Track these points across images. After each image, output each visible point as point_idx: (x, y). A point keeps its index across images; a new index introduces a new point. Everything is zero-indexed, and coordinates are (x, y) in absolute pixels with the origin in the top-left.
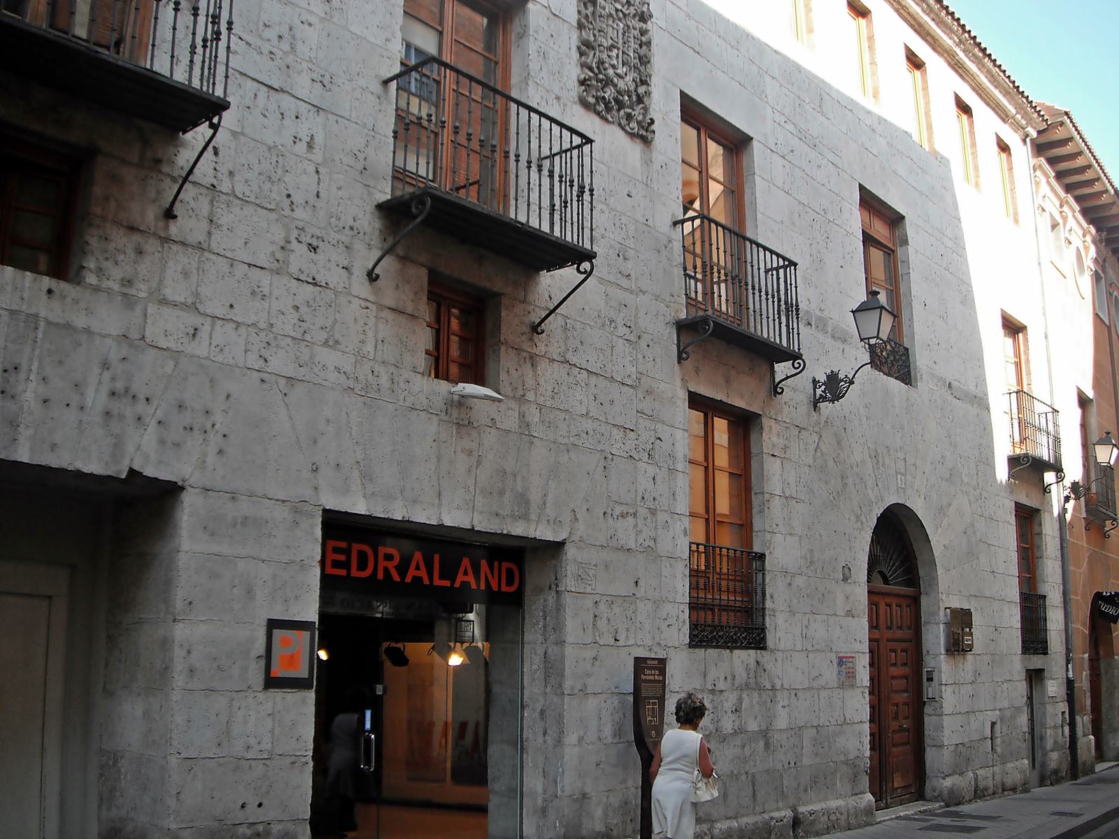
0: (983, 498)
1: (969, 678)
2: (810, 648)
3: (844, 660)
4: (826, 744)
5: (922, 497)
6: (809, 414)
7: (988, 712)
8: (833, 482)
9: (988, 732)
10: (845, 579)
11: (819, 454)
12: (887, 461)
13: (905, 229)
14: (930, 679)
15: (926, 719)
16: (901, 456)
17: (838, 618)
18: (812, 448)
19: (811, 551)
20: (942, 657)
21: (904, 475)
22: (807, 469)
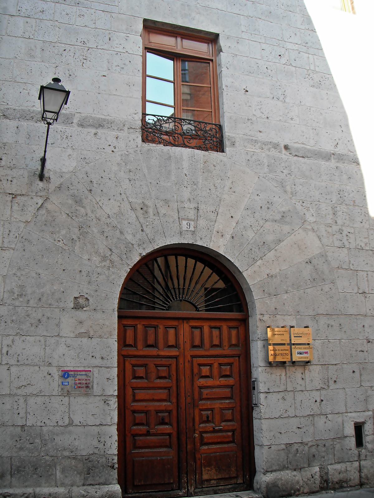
0: (345, 233)
1: (317, 384)
2: (13, 362)
3: (70, 373)
4: (38, 441)
5: (228, 237)
6: (31, 184)
7: (349, 414)
8: (63, 232)
9: (350, 431)
10: (77, 307)
11: (43, 212)
12: (162, 211)
13: (219, 43)
14: (254, 388)
15: (254, 421)
16: (193, 205)
17: (63, 339)
18: (32, 209)
19: (22, 287)
20: (260, 369)
21: (196, 220)
22: (22, 225)
